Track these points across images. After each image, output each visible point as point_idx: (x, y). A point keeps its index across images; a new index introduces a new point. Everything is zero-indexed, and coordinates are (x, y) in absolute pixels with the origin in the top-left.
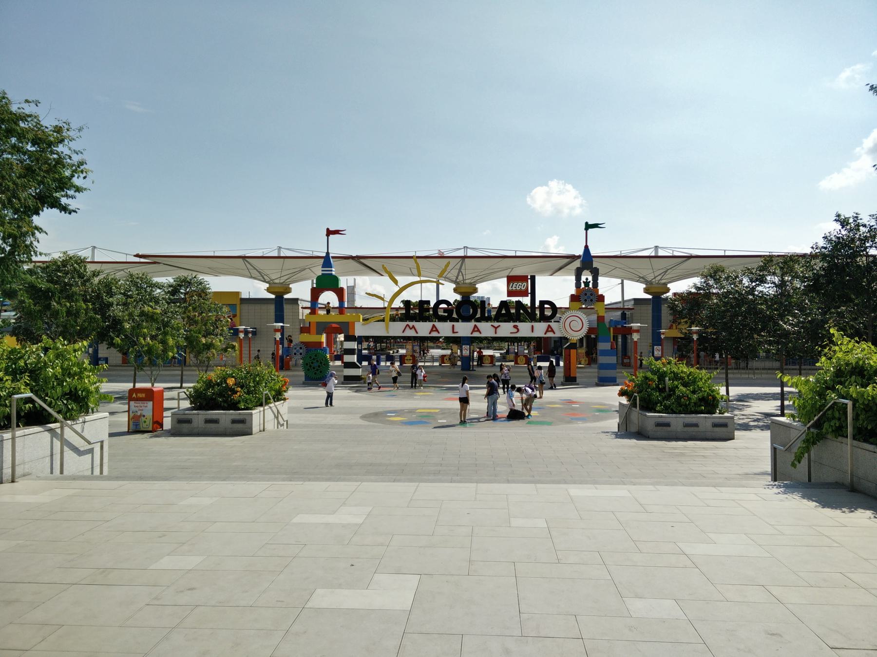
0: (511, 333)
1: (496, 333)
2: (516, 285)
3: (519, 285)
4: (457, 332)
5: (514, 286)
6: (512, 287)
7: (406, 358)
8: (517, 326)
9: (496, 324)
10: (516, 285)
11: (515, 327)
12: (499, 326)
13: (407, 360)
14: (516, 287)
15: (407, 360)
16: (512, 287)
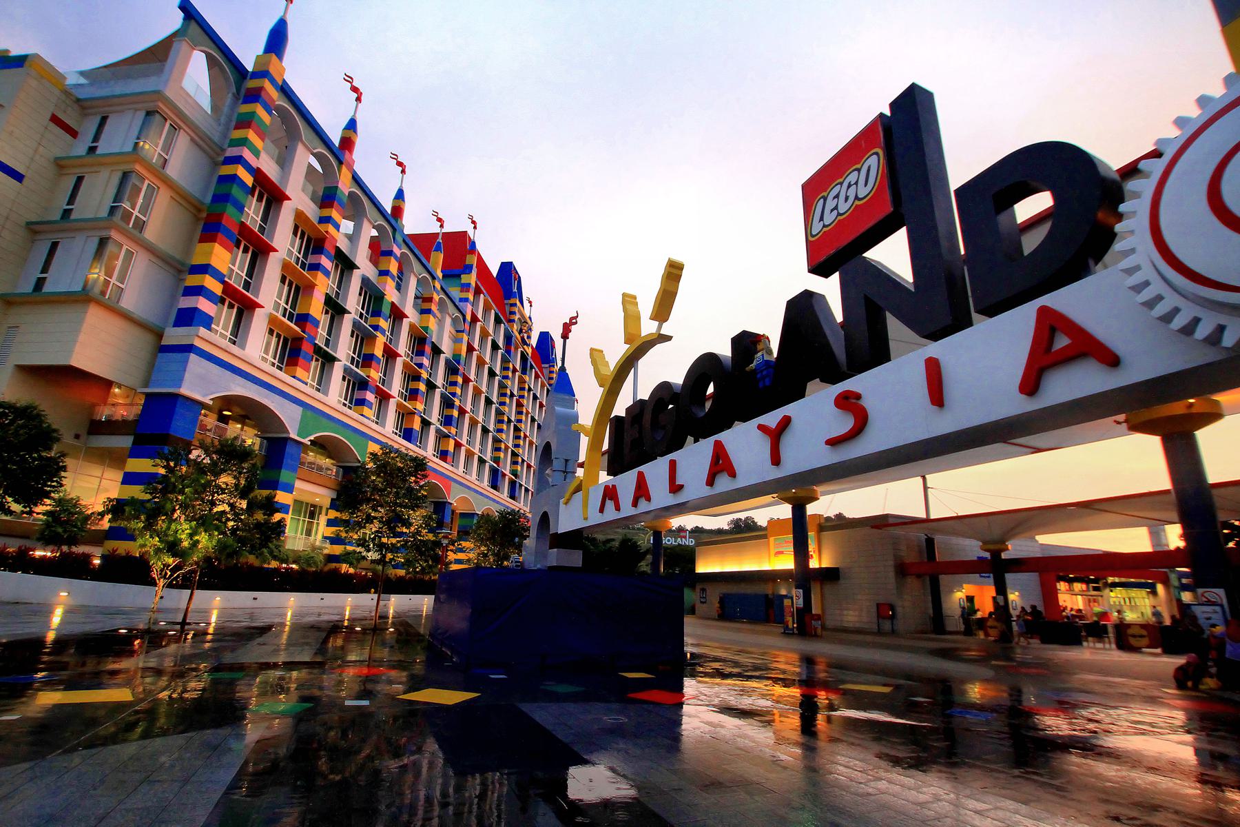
0: (833, 442)
1: (776, 460)
2: (837, 196)
3: (849, 186)
4: (681, 487)
5: (831, 204)
6: (822, 219)
7: (1130, 631)
8: (858, 396)
9: (771, 419)
10: (837, 196)
11: (849, 402)
12: (786, 422)
13: (1134, 636)
14: (836, 208)
15: (1134, 636)
16: (822, 219)
